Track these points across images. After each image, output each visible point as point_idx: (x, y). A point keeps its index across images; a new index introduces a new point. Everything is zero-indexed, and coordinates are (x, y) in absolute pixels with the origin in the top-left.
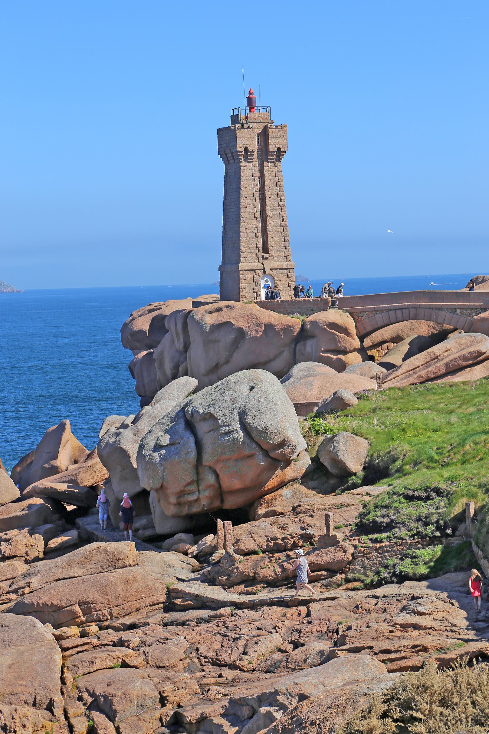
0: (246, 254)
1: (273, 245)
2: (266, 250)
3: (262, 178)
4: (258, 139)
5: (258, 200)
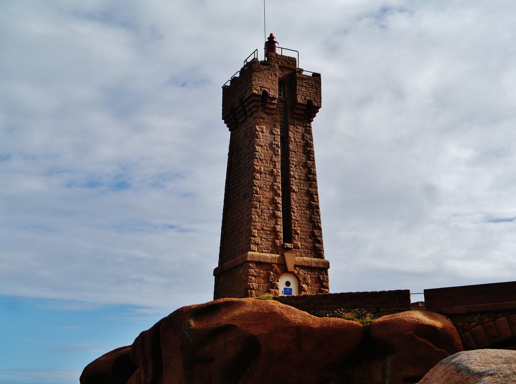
0: (258, 240)
1: (299, 232)
2: (289, 236)
3: (285, 139)
4: (280, 91)
5: (279, 166)
